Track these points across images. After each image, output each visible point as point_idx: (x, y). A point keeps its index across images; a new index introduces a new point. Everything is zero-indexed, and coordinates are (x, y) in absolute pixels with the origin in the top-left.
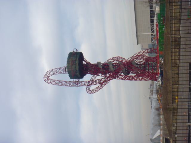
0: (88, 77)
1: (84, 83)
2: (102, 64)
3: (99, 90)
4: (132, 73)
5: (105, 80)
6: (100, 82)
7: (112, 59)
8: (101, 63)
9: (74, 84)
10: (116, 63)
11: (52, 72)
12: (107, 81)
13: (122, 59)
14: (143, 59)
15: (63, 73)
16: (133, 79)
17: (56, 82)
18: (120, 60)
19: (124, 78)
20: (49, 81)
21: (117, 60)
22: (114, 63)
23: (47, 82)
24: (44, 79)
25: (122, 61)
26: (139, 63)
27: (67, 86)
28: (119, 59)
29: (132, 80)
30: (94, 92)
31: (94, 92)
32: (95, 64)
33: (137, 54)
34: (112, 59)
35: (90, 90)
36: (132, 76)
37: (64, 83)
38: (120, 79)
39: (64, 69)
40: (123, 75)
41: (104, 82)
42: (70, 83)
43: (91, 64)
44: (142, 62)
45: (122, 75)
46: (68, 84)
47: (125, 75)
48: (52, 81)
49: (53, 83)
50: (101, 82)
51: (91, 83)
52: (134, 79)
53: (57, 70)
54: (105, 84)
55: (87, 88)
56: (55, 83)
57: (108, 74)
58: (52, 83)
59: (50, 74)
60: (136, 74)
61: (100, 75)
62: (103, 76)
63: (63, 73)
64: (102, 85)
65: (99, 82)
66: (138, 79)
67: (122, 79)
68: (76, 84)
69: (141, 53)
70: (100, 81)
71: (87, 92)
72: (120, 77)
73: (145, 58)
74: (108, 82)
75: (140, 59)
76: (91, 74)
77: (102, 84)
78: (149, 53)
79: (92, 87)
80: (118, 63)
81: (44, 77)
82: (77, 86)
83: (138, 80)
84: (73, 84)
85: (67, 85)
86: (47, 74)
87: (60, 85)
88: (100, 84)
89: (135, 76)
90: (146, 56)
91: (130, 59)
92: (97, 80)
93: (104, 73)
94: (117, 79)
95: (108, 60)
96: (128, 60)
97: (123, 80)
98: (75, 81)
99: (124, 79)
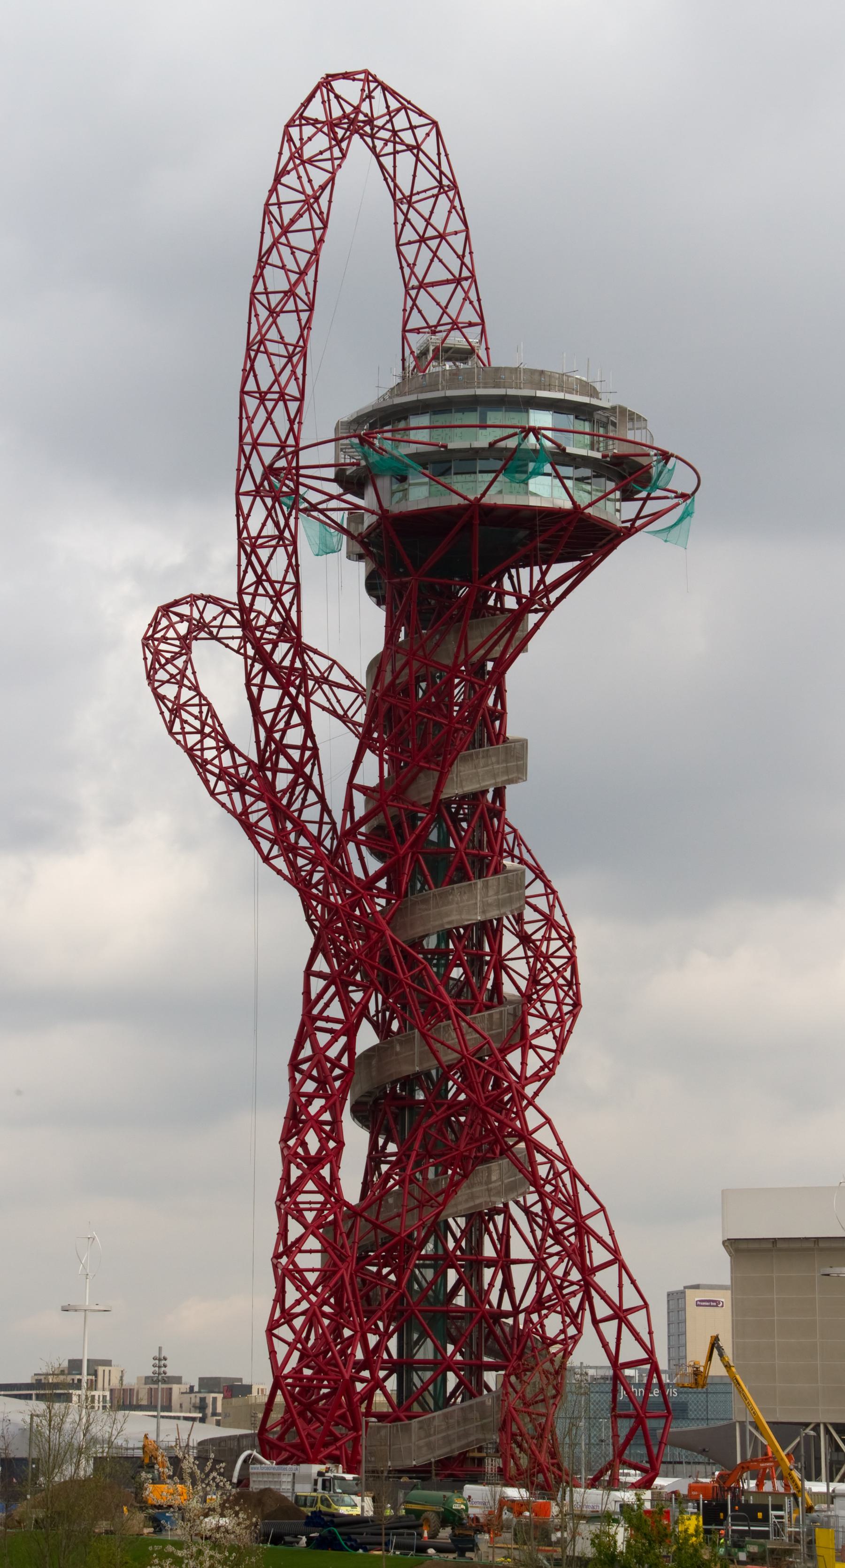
1: (277, 569)
2: (499, 793)
3: (190, 751)
4: (375, 1156)
5: (301, 828)
6: (283, 763)
7: (549, 921)
8: (510, 791)
9: (268, 454)
10: (500, 965)
11: (425, 181)
12: (290, 851)
13: (547, 1041)
14: (539, 1304)
15: (415, 321)
16: (295, 1173)
17: (304, 222)
18: (535, 1024)
19: (319, 1053)
20: (321, 141)
21: (533, 980)
22: (509, 941)
23: (300, 119)
24: (346, 76)
25: (525, 1043)
26: (489, 1251)
27: (251, 360)
28: (551, 1009)
29: (289, 1157)
30: (170, 691)
31: (170, 691)
32: (502, 716)
33: (597, 1224)
34: (549, 921)
35: (185, 643)
36: (334, 1157)
37: (289, 326)
38: (309, 1003)
39: (456, 339)
40: (350, 1047)
41: (277, 812)
42: (282, 396)
43: (503, 664)
44: (508, 1285)
45: (351, 1030)
46: (266, 378)
47: (348, 1073)
48: (319, 177)
49: (285, 194)
50: (283, 781)
52: (301, 1180)
53: (445, 252)
54: (251, 830)
55: (212, 611)
56: (289, 212)
57: (374, 865)
58: (290, 179)
59: (406, 160)
60: (355, 1212)
62: (349, 806)
63: (415, 321)
64: (241, 786)
65: (282, 749)
66: (295, 1230)
67: (306, 1032)
68: (270, 471)
69: (606, 1279)
70: (297, 769)
71: (166, 610)
72: (336, 1010)
73: (553, 1324)
74: (280, 863)
75: (539, 1264)
76: (377, 667)
78: (617, 1378)
80: (508, 989)
81: (369, 77)
82: (248, 485)
83: (283, 1233)
84: (268, 436)
85: (261, 361)
86: (400, 121)
87: (259, 276)
88: (259, 768)
89: (330, 1189)
90: (575, 1339)
91: (544, 1137)
92: (309, 734)
94: (309, 973)
95: (539, 874)
96: (532, 1118)
97: (299, 1046)
98: (305, 458)
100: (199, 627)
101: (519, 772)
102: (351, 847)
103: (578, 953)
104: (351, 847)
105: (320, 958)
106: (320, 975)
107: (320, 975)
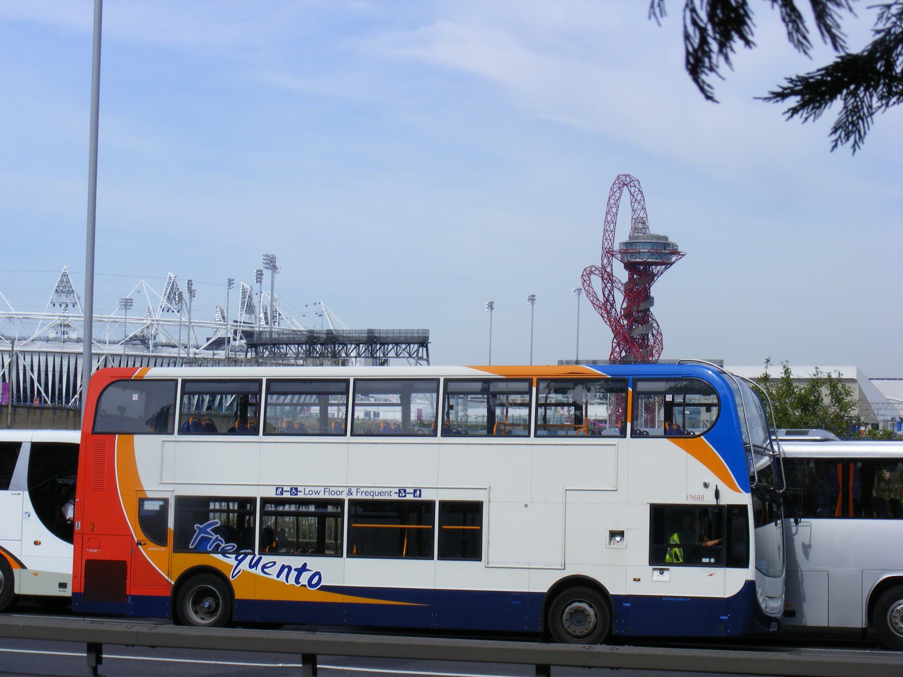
0: (622, 274)
10: (648, 340)
22: (650, 335)
25: (652, 355)
41: (608, 313)
51: (608, 278)
61: (625, 305)
67: (612, 353)
74: (608, 323)
77: (606, 307)
79: (597, 282)
93: (627, 314)
99: (612, 357)
100: (591, 272)
101: (652, 304)
102: (621, 320)
103: (663, 339)
104: (621, 320)
105: (615, 339)
106: (615, 343)
107: (615, 343)
